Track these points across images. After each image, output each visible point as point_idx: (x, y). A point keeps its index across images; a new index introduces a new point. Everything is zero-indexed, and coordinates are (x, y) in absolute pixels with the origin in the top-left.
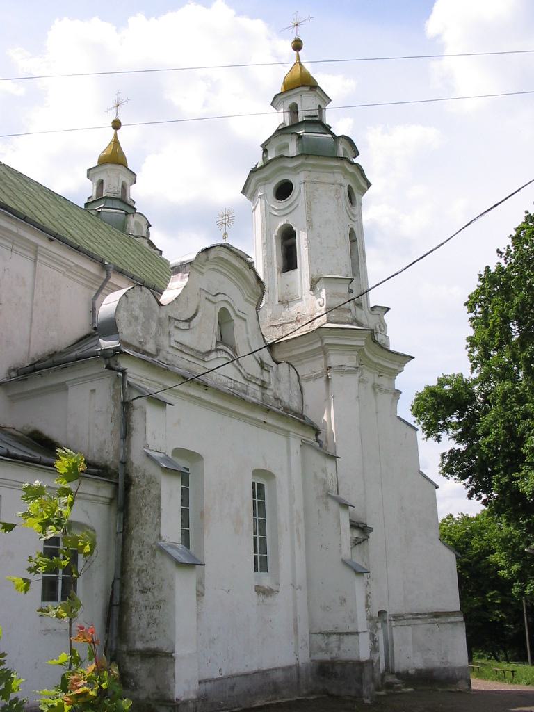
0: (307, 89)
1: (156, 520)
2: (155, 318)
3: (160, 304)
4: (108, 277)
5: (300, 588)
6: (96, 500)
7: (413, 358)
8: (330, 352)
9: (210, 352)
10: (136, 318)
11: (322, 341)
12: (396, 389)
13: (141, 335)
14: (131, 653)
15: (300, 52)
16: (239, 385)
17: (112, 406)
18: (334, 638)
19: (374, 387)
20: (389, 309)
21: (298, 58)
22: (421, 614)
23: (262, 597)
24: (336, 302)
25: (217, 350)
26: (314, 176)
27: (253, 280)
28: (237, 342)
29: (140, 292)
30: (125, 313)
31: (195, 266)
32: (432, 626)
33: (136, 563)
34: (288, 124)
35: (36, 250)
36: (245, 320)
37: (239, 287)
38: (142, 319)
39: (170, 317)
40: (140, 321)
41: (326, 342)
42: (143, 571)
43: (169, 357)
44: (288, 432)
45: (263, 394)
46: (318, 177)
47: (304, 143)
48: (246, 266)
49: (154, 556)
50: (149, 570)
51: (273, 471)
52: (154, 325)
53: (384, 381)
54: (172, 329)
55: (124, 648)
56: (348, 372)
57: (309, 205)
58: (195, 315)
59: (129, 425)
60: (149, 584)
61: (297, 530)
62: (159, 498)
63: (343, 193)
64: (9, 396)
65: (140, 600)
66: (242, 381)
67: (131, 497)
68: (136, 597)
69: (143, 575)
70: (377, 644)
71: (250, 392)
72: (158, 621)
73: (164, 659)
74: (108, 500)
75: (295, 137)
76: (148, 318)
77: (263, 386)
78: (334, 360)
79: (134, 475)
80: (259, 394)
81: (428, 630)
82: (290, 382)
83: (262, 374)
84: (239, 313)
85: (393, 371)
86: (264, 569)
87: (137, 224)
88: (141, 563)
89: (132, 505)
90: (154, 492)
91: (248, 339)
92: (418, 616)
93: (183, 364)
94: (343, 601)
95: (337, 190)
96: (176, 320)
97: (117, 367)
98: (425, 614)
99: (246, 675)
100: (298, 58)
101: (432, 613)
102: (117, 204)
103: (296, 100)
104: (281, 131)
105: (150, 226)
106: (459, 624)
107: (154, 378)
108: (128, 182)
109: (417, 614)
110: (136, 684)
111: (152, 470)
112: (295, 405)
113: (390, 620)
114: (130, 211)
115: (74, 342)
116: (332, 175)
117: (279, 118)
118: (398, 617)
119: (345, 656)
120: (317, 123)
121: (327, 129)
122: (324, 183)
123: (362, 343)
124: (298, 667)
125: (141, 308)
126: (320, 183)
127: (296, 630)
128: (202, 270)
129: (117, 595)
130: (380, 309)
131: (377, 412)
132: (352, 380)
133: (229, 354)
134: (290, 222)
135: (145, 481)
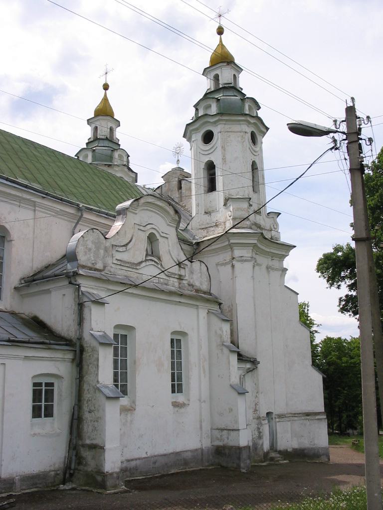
0: (225, 64)
1: (96, 372)
2: (103, 247)
3: (106, 238)
4: (82, 215)
5: (204, 401)
6: (63, 360)
7: (295, 247)
8: (234, 248)
9: (141, 262)
10: (90, 250)
11: (229, 241)
12: (284, 267)
13: (93, 259)
14: (83, 446)
15: (222, 36)
17: (74, 305)
19: (268, 268)
20: (280, 214)
21: (221, 41)
22: (297, 414)
23: (177, 409)
25: (146, 260)
26: (227, 126)
27: (172, 212)
28: (161, 253)
29: (92, 233)
30: (83, 248)
31: (131, 210)
32: (305, 421)
33: (86, 396)
34: (213, 90)
35: (34, 204)
36: (167, 238)
37: (162, 217)
38: (94, 249)
39: (113, 245)
40: (92, 251)
41: (232, 241)
42: (90, 400)
43: (112, 270)
44: (197, 306)
45: (180, 283)
46: (230, 128)
47: (221, 104)
48: (166, 204)
49: (95, 392)
50: (93, 400)
51: (186, 331)
52: (102, 252)
53: (275, 263)
54: (114, 252)
55: (80, 443)
56: (246, 261)
57: (223, 148)
58: (130, 241)
59: (83, 317)
60: (93, 408)
61: (203, 367)
62: (98, 360)
63: (247, 138)
64: (21, 295)
65: (88, 417)
67: (84, 359)
68: (86, 415)
69: (90, 402)
70: (261, 434)
71: (170, 283)
72: (97, 428)
73: (100, 450)
74: (71, 360)
75: (215, 100)
76: (98, 248)
77: (180, 278)
78: (238, 253)
79: (85, 345)
80: (177, 284)
81: (302, 424)
83: (180, 270)
84: (162, 235)
86: (180, 391)
87: (120, 156)
88: (89, 396)
89: (84, 363)
90: (96, 356)
91: (169, 249)
92: (295, 415)
93: (121, 273)
94: (231, 410)
96: (116, 246)
97: (75, 283)
98: (300, 414)
99: (165, 455)
100: (221, 41)
101: (305, 413)
102: (106, 143)
103: (218, 72)
104: (207, 96)
105: (129, 156)
106: (323, 420)
107: (101, 285)
108: (114, 127)
109: (295, 414)
110: (86, 463)
111: (94, 343)
112: (205, 287)
113: (276, 418)
114: (115, 147)
115: (61, 257)
116: (239, 125)
117: (206, 84)
118: (281, 416)
119: (231, 443)
120: (233, 88)
121: (239, 92)
122: (234, 132)
123: (256, 242)
124: (202, 449)
125: (93, 242)
126: (231, 132)
127: (201, 428)
128: (136, 212)
129: (76, 413)
131: (269, 284)
132: (249, 265)
133: (155, 262)
134: (213, 159)
135: (91, 349)
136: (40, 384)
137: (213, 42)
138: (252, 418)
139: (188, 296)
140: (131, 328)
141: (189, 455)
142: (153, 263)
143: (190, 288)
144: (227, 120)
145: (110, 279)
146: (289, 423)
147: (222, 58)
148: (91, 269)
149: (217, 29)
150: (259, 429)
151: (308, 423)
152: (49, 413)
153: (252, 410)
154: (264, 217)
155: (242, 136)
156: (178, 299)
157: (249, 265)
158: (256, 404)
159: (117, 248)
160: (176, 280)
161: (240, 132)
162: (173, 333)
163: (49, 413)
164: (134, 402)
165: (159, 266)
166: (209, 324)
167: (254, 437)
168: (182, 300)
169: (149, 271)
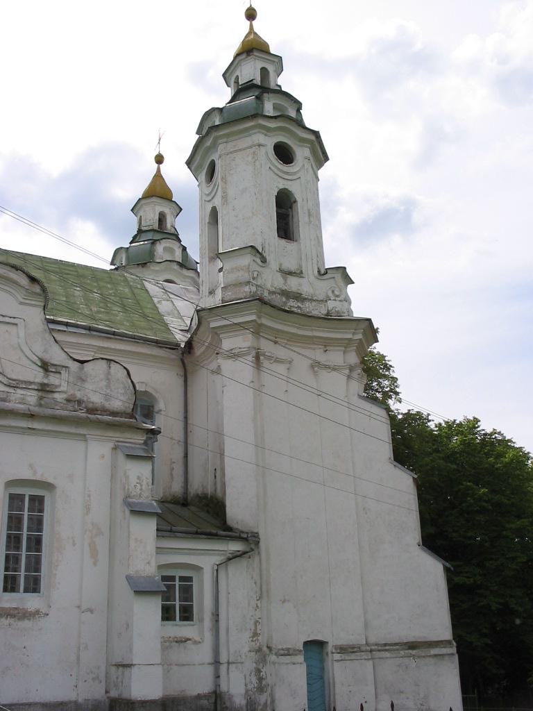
5: (91, 611)
19: (316, 366)
24: (232, 278)
27: (24, 281)
32: (406, 661)
36: (16, 324)
41: (213, 325)
44: (85, 435)
45: (41, 398)
48: (9, 268)
51: (50, 480)
70: (264, 683)
81: (399, 666)
82: (108, 379)
85: (346, 342)
91: (19, 344)
92: (386, 647)
98: (396, 644)
106: (447, 658)
109: (385, 645)
113: (333, 653)
122: (240, 150)
126: (235, 151)
130: (334, 271)
137: (241, 28)
138: (247, 649)
139: (51, 418)
143: (70, 406)
144: (228, 135)
146: (371, 662)
147: (253, 48)
149: (247, 10)
150: (258, 671)
151: (412, 663)
153: (248, 634)
154: (312, 278)
155: (254, 152)
156: (24, 424)
158: (256, 622)
160: (35, 393)
161: (251, 147)
162: (10, 484)
166: (114, 467)
167: (249, 687)
168: (36, 425)
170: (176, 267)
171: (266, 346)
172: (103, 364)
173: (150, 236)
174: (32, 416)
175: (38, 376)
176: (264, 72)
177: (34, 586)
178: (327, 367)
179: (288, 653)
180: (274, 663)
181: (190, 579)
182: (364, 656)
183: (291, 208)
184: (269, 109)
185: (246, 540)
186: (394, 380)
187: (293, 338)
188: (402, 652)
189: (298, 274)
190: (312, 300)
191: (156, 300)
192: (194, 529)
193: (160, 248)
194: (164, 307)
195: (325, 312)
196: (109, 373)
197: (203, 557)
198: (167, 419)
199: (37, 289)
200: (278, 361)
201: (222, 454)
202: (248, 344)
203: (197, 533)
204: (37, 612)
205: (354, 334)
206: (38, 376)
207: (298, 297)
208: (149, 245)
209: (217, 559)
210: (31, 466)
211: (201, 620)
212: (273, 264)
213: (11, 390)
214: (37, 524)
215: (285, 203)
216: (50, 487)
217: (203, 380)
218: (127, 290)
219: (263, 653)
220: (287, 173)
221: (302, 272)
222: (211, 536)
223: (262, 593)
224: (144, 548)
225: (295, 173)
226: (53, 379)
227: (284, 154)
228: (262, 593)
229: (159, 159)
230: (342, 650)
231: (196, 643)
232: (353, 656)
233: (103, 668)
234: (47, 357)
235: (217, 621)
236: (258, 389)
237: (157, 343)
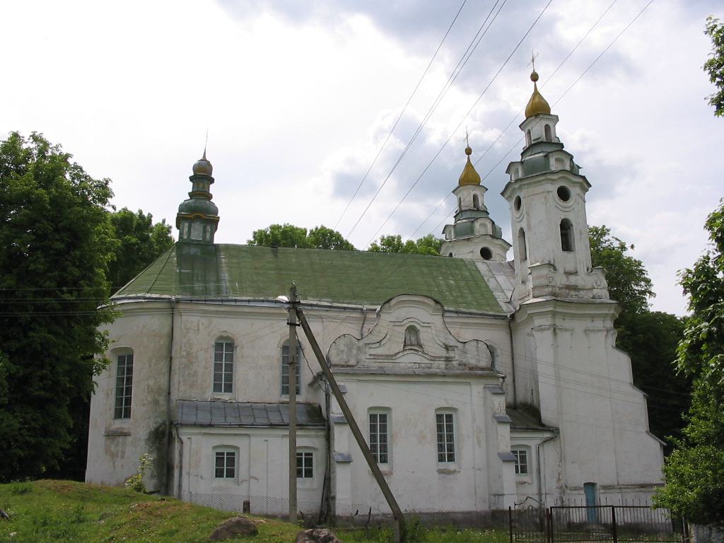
0: (533, 118)
5: (479, 469)
6: (317, 436)
10: (342, 351)
16: (423, 365)
18: (497, 497)
19: (586, 331)
24: (538, 282)
25: (403, 351)
26: (531, 190)
27: (432, 303)
37: (426, 311)
41: (529, 312)
43: (365, 364)
45: (447, 365)
51: (455, 407)
52: (354, 351)
54: (367, 349)
56: (544, 330)
61: (478, 438)
66: (428, 361)
83: (448, 353)
92: (629, 486)
93: (374, 365)
95: (545, 197)
98: (634, 485)
109: (628, 485)
118: (607, 488)
119: (501, 508)
122: (537, 194)
125: (345, 345)
126: (535, 194)
136: (301, 454)
140: (388, 409)
141: (460, 516)
142: (412, 351)
144: (529, 184)
145: (356, 372)
146: (620, 494)
148: (343, 366)
152: (309, 474)
153: (555, 479)
157: (549, 333)
158: (559, 474)
159: (370, 346)
161: (543, 193)
163: (309, 474)
164: (392, 469)
165: (420, 353)
166: (485, 398)
169: (410, 360)
170: (489, 238)
171: (559, 322)
172: (475, 343)
173: (469, 215)
174: (444, 376)
175: (443, 353)
176: (547, 128)
177: (451, 458)
178: (593, 331)
179: (576, 489)
180: (569, 494)
181: (525, 452)
182: (617, 491)
183: (569, 228)
184: (554, 165)
185: (552, 431)
186: (648, 281)
187: (573, 316)
188: (637, 489)
189: (576, 273)
190: (584, 289)
191: (486, 279)
192: (525, 427)
193: (477, 225)
194: (492, 284)
195: (592, 296)
196: (478, 347)
197: (531, 441)
198: (503, 364)
199: (439, 307)
200: (566, 330)
201: (537, 382)
202: (549, 323)
203: (527, 429)
204: (455, 471)
205: (609, 310)
206: (443, 353)
207: (575, 288)
208: (469, 224)
209: (538, 442)
210: (446, 400)
211: (531, 473)
212: (561, 270)
213: (432, 362)
214: (450, 428)
215: (565, 227)
216: (455, 410)
217: (521, 336)
218: (467, 274)
219: (563, 489)
220: (565, 207)
221: (577, 272)
222: (535, 430)
223: (562, 458)
224: (505, 438)
225: (569, 207)
226: (451, 354)
227: (564, 194)
228: (562, 458)
229: (468, 151)
230: (605, 487)
231: (529, 484)
232: (610, 491)
233: (487, 497)
234: (447, 342)
235: (540, 473)
236: (556, 346)
237: (495, 317)
